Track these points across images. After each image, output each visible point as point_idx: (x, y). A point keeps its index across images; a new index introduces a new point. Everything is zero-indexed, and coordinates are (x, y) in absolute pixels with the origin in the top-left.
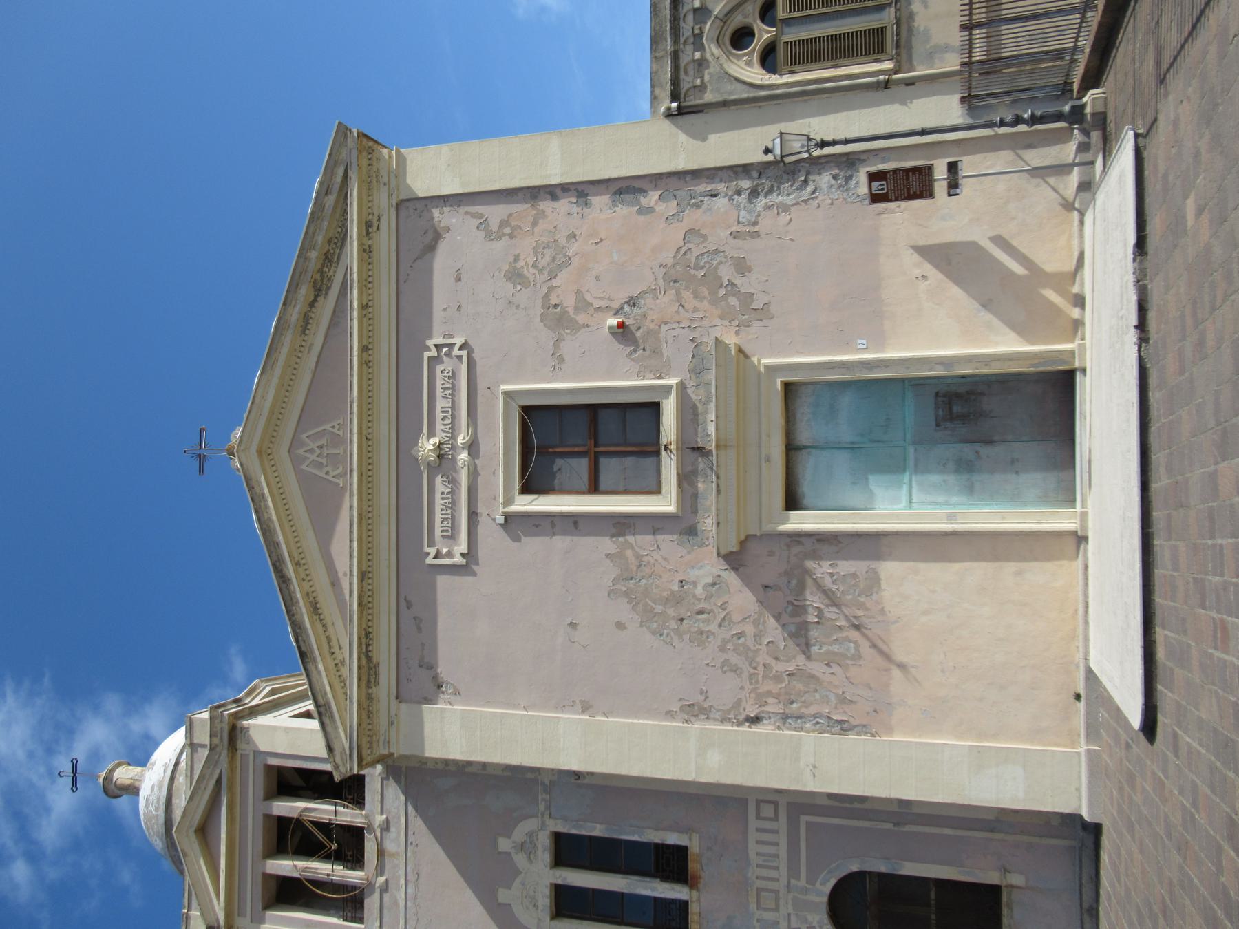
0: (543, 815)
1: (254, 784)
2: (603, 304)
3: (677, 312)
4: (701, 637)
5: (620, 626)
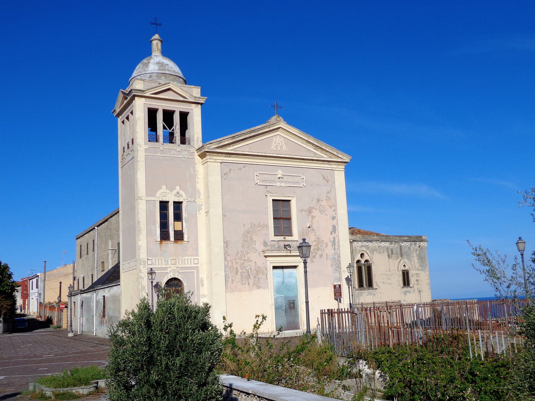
0: (187, 199)
1: (184, 108)
2: (313, 223)
3: (312, 241)
4: (243, 246)
5: (244, 225)
